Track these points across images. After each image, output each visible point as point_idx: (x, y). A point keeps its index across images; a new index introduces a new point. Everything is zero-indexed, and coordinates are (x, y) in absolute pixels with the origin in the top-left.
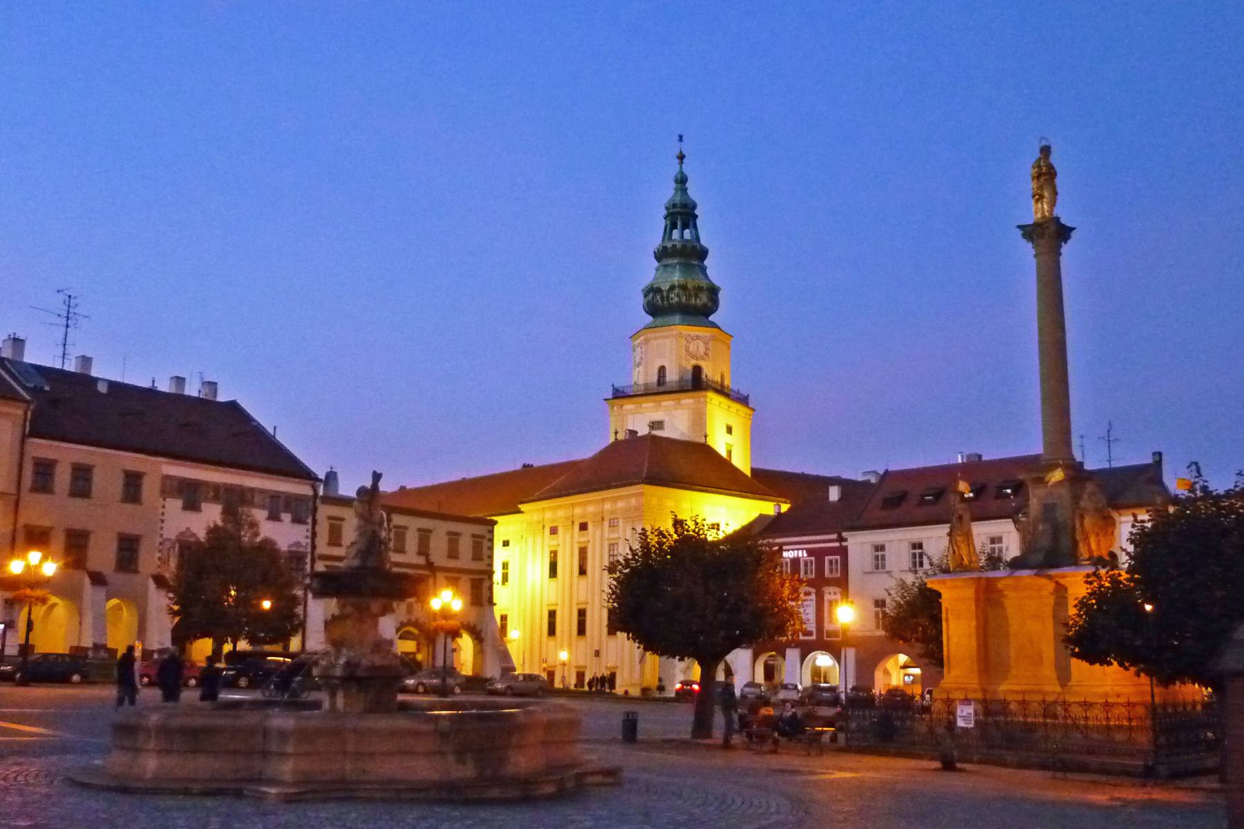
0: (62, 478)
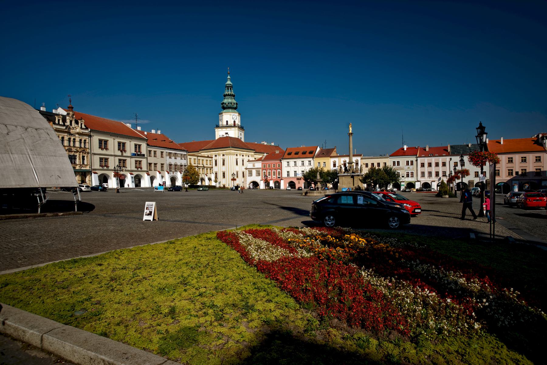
0: (152, 153)
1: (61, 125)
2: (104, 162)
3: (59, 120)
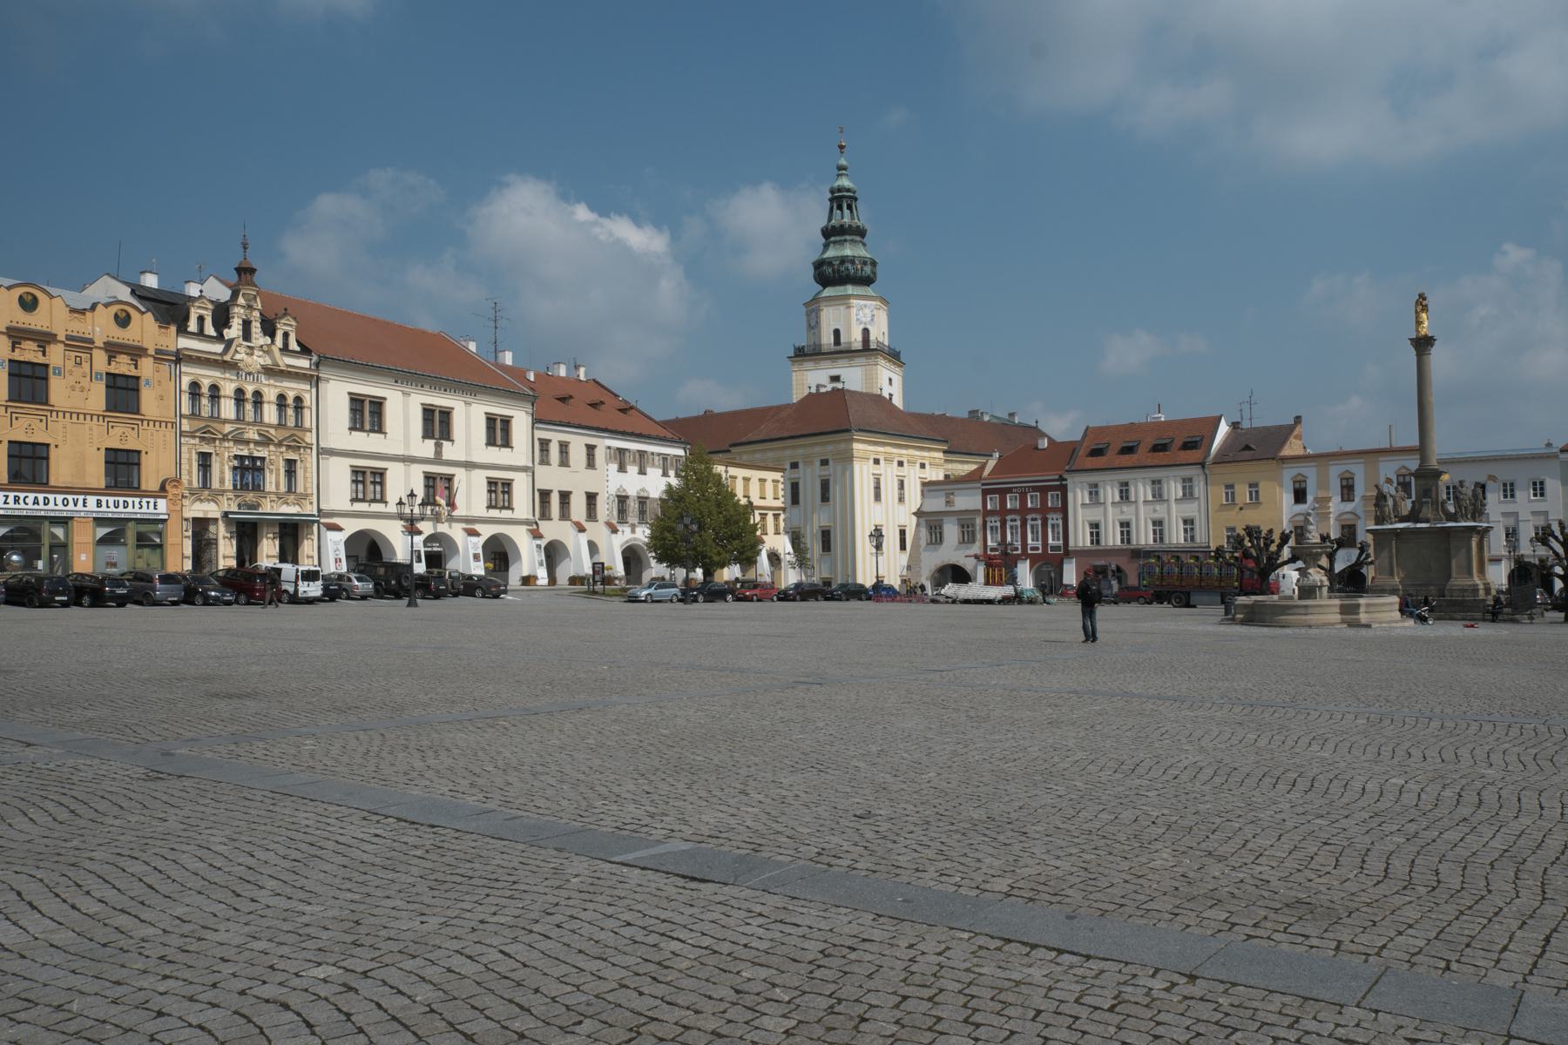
1: (209, 339)
2: (368, 481)
3: (201, 319)
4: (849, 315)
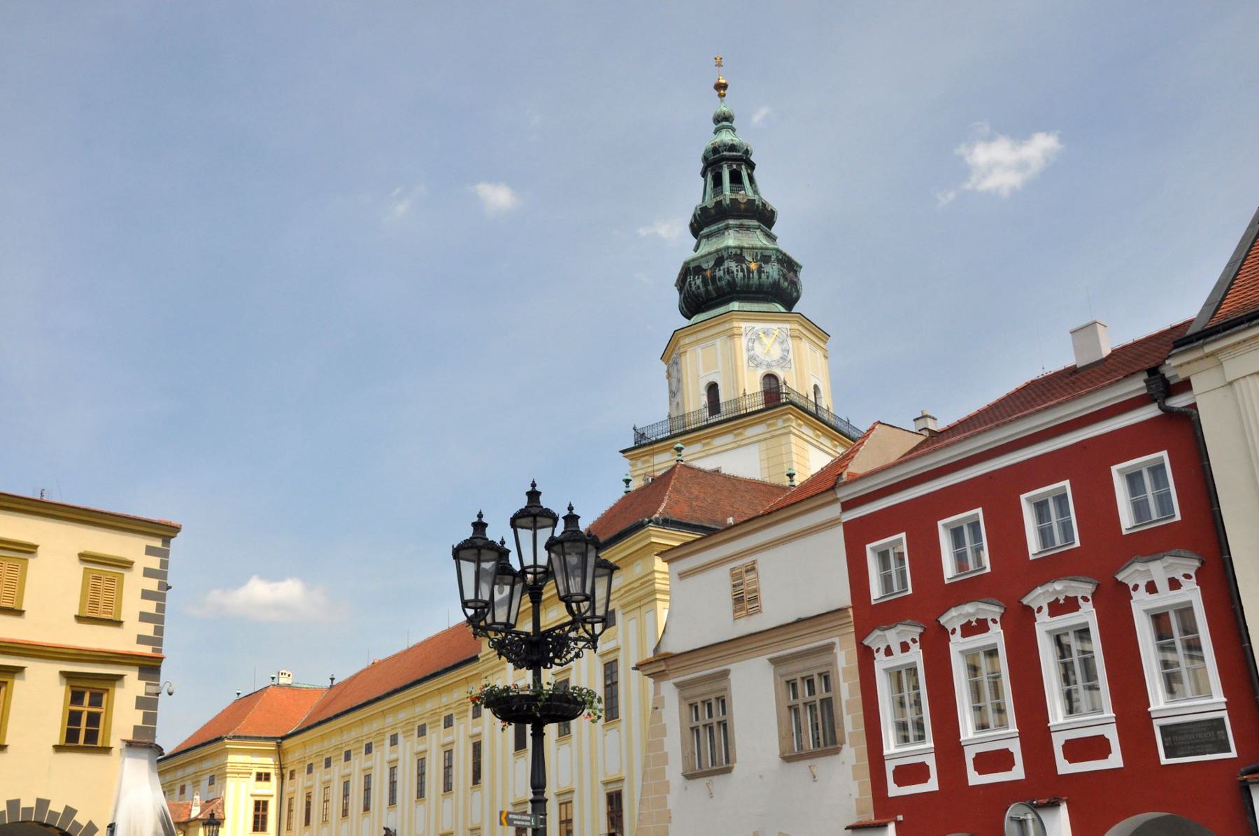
4: (733, 350)
